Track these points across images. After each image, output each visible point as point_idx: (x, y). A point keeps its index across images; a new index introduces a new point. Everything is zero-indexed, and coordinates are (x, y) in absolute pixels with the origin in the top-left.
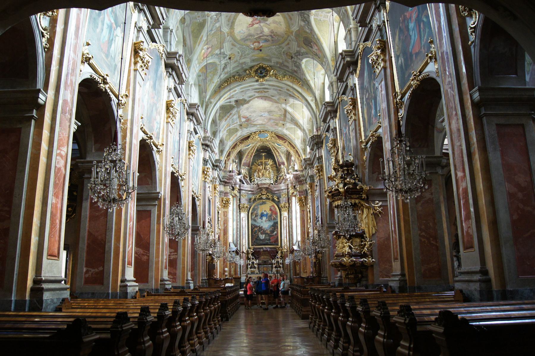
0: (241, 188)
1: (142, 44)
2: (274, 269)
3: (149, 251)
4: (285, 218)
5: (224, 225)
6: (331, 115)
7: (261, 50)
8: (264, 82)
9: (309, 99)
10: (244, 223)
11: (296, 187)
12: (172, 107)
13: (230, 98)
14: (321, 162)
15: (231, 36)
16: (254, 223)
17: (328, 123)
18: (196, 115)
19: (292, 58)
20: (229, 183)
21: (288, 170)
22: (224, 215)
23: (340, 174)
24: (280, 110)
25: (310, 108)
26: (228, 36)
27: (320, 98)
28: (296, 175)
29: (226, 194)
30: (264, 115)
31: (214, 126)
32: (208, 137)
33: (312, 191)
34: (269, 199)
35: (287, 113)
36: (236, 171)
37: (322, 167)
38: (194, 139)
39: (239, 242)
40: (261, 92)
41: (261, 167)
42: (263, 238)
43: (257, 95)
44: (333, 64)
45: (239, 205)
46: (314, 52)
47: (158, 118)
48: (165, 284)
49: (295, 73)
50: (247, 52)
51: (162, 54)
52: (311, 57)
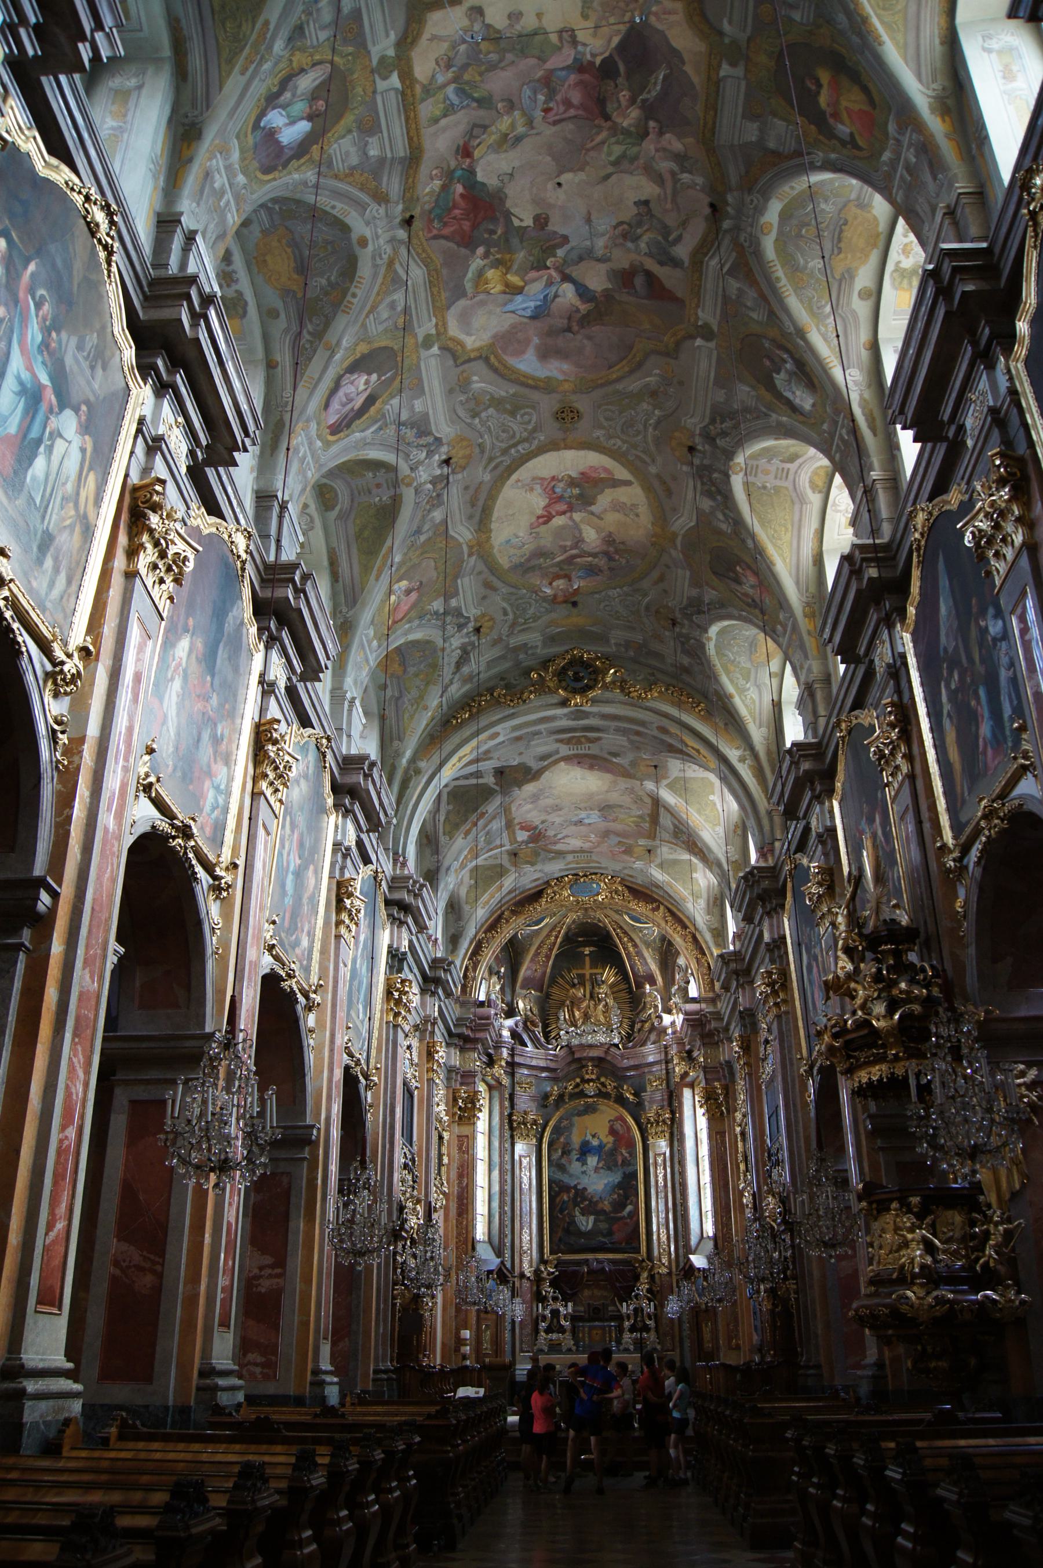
0: (517, 1059)
1: (158, 488)
2: (627, 1337)
3: (162, 1254)
4: (660, 1160)
5: (460, 1183)
6: (813, 790)
7: (575, 604)
8: (587, 708)
9: (733, 754)
10: (527, 1176)
11: (695, 1054)
12: (275, 742)
13: (477, 760)
14: (781, 957)
15: (481, 557)
16: (559, 1176)
17: (804, 817)
18: (364, 795)
19: (674, 624)
20: (476, 1041)
21: (667, 998)
22: (460, 1148)
23: (868, 968)
24: (638, 800)
25: (736, 786)
26: (470, 555)
27: (769, 753)
28: (696, 1013)
29: (467, 1077)
30: (587, 821)
31: (428, 852)
32: (409, 877)
33: (752, 1061)
34: (606, 1096)
35: (662, 810)
36: (499, 1002)
37: (784, 973)
38: (360, 877)
39: (508, 1241)
40: (578, 741)
41: (580, 994)
43: (565, 750)
44: (811, 627)
45: (510, 1115)
46: (746, 595)
47: (221, 772)
48: (216, 1388)
49: (685, 677)
50: (531, 611)
51: (244, 562)
52: (736, 613)
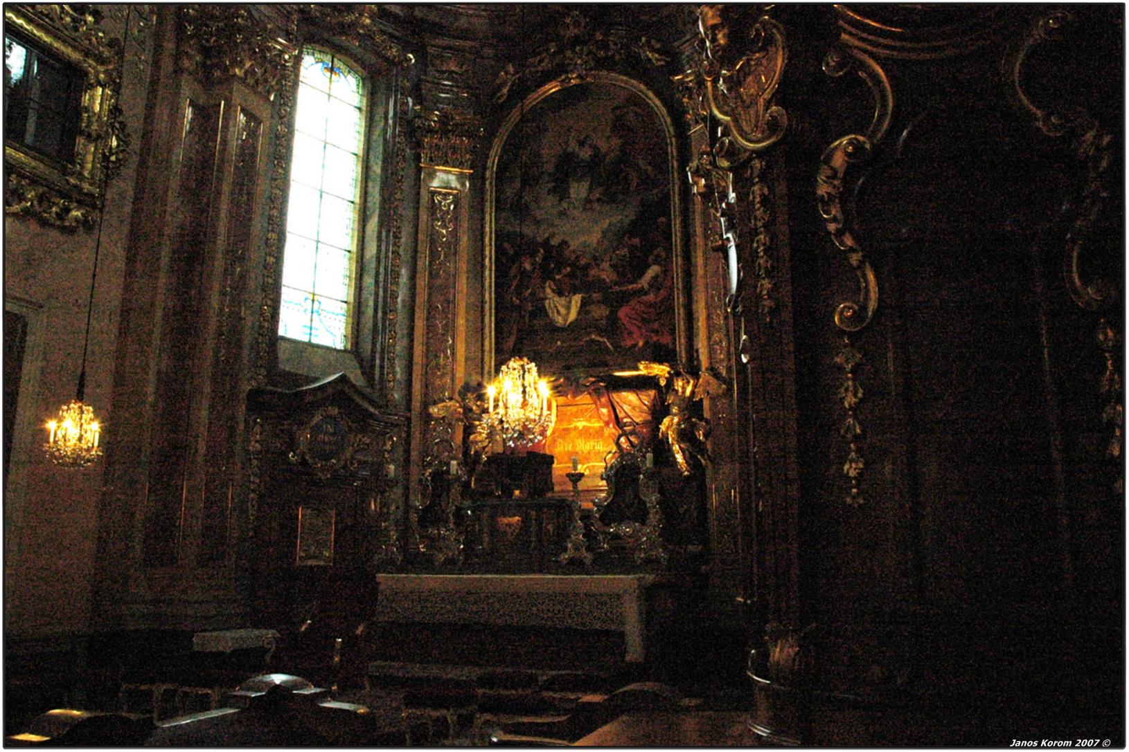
16: (513, 227)
42: (573, 316)
